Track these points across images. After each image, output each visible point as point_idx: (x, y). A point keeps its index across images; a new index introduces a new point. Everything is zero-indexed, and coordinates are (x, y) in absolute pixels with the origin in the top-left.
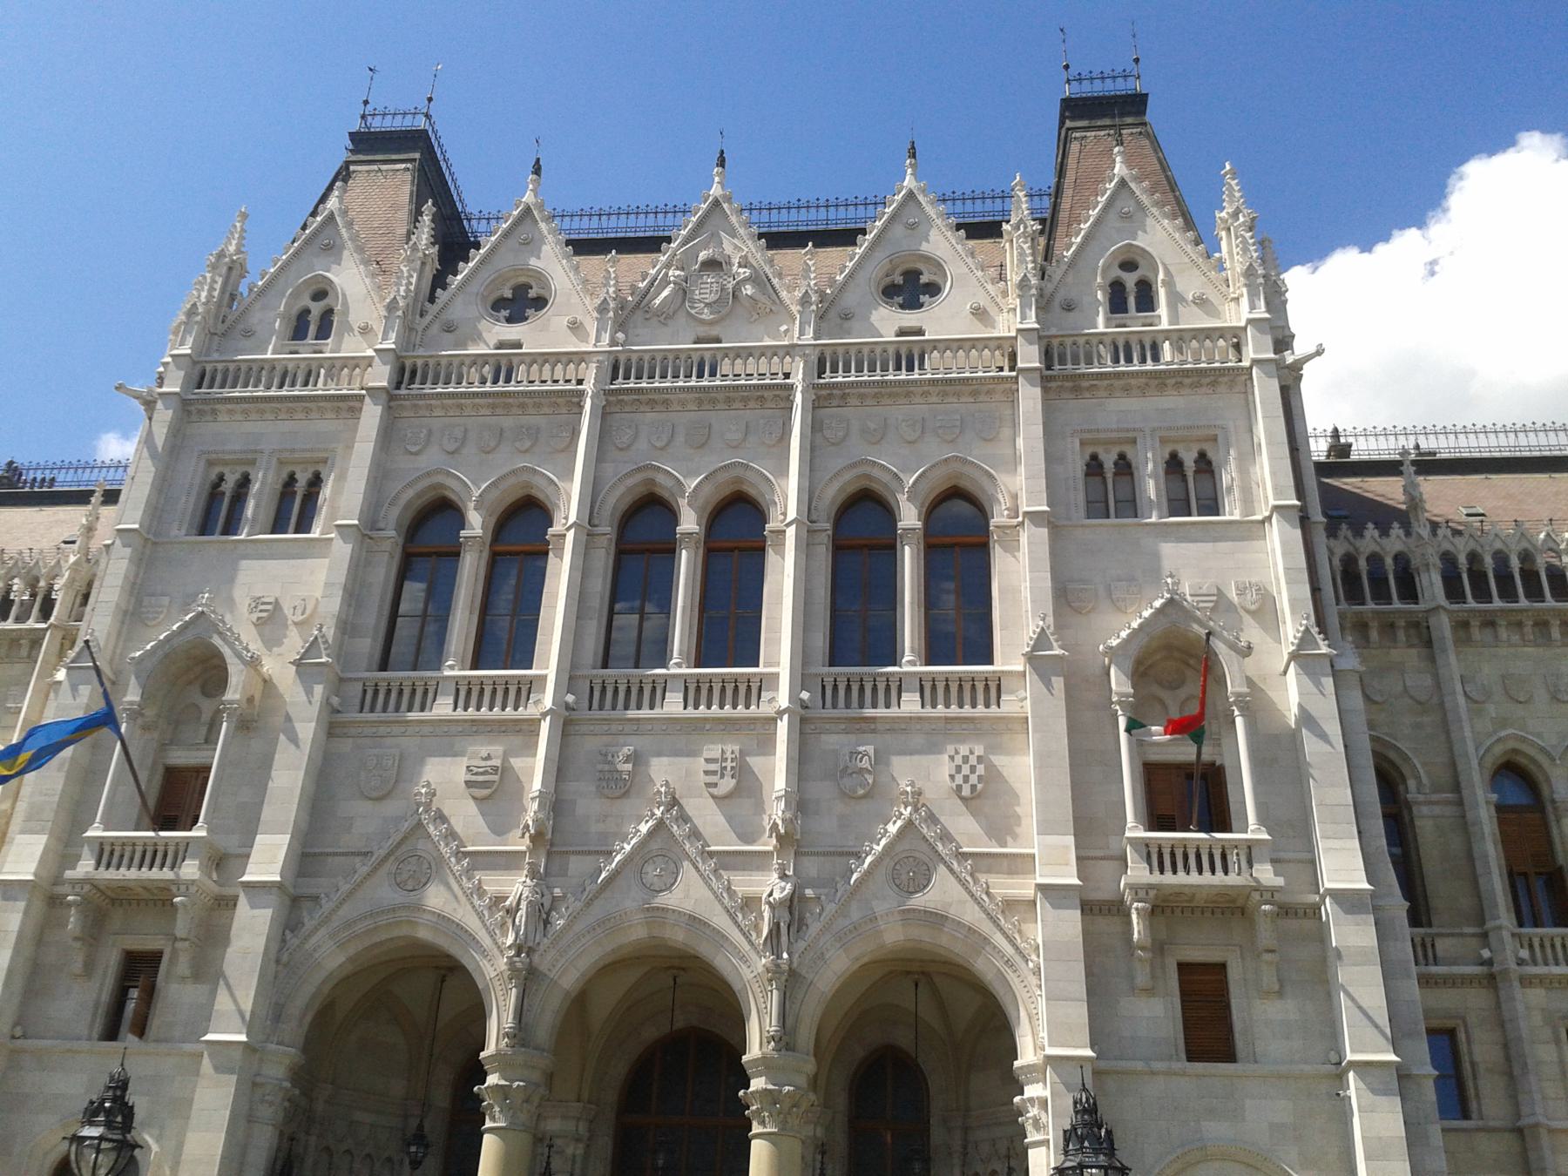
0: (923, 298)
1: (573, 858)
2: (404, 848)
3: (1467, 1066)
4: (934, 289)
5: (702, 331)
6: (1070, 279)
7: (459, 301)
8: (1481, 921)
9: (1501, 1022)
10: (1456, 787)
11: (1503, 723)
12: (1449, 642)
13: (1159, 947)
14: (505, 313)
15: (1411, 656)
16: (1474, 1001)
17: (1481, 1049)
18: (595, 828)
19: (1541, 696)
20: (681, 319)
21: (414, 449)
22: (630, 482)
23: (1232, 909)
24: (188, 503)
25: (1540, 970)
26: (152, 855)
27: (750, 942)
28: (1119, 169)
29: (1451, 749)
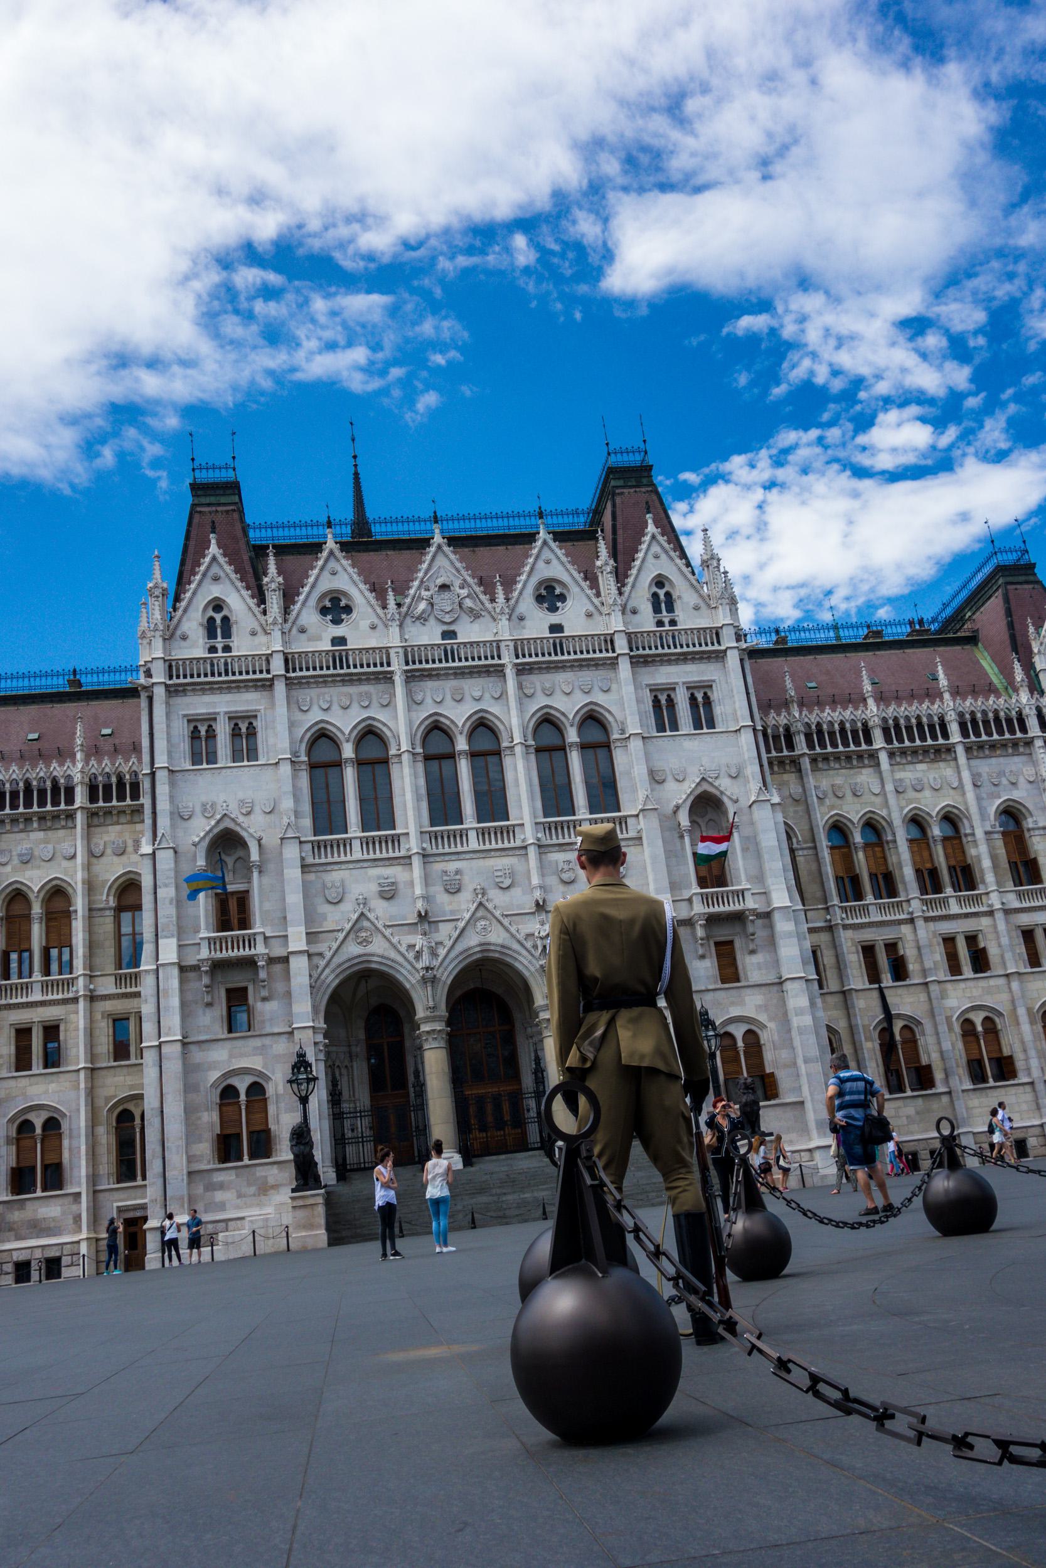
0: (559, 604)
1: (440, 924)
2: (357, 926)
3: (821, 967)
4: (562, 598)
5: (445, 628)
6: (633, 595)
7: (304, 613)
8: (826, 903)
9: (835, 945)
10: (814, 840)
11: (832, 807)
12: (809, 772)
13: (708, 938)
14: (329, 617)
15: (791, 778)
16: (823, 938)
17: (828, 959)
18: (448, 908)
19: (849, 794)
20: (432, 621)
21: (305, 708)
22: (427, 722)
23: (738, 918)
24: (184, 746)
25: (850, 921)
26: (236, 942)
27: (532, 955)
28: (651, 528)
29: (810, 821)
